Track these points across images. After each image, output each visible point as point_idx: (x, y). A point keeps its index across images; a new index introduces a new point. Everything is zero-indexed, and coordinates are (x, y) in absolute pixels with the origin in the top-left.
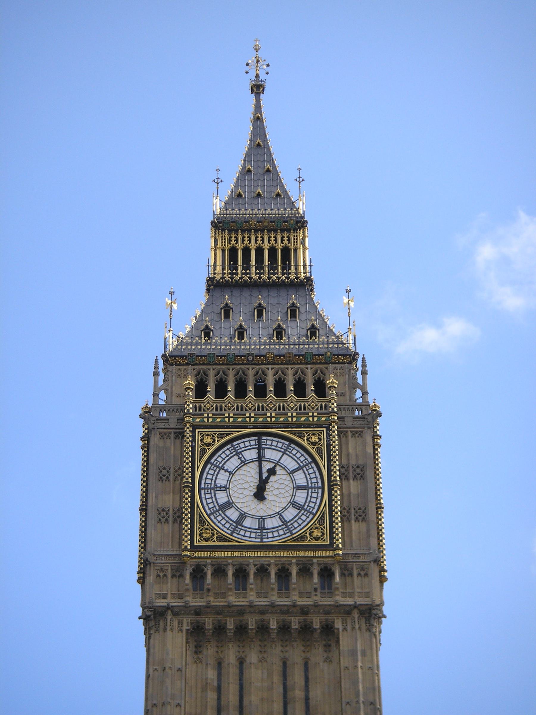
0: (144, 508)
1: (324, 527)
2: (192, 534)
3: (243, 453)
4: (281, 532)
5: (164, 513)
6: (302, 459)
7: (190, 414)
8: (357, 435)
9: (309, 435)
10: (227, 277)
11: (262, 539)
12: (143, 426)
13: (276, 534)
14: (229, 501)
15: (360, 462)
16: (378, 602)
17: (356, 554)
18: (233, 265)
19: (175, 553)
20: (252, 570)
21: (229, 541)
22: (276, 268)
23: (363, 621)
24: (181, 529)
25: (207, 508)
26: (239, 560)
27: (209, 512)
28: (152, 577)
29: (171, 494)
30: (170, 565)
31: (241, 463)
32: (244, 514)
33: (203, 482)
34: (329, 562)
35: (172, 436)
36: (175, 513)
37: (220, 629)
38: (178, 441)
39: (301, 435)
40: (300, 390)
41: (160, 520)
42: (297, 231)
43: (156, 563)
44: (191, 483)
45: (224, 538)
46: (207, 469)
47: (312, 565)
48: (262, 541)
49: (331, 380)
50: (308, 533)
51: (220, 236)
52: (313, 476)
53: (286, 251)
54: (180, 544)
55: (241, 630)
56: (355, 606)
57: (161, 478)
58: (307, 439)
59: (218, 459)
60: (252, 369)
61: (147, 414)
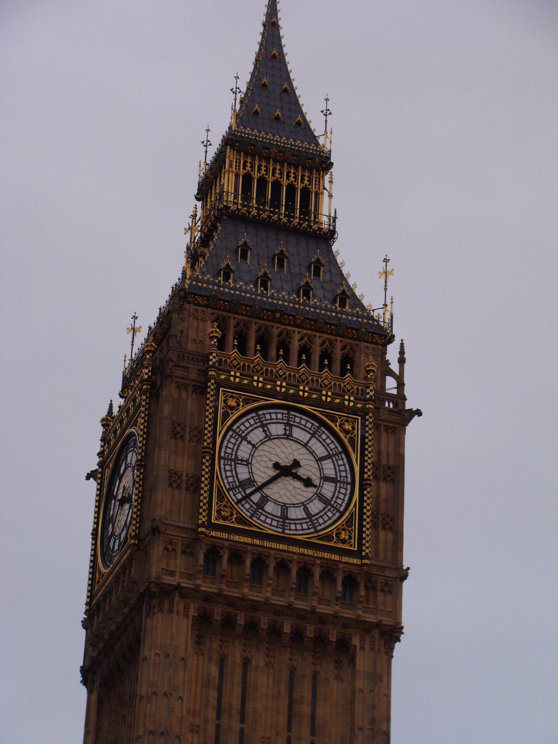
1: (352, 530)
2: (210, 509)
3: (268, 426)
4: (305, 526)
6: (332, 446)
8: (390, 431)
9: (341, 421)
10: (285, 220)
11: (284, 529)
13: (299, 527)
14: (250, 479)
15: (391, 463)
17: (381, 566)
18: (246, 197)
19: (186, 526)
22: (293, 211)
23: (382, 642)
28: (160, 549)
31: (266, 437)
32: (266, 497)
33: (223, 450)
35: (190, 388)
36: (188, 480)
37: (228, 622)
42: (320, 172)
43: (165, 534)
44: (212, 449)
45: (244, 521)
46: (228, 437)
47: (336, 570)
48: (283, 532)
50: (334, 533)
52: (342, 468)
53: (306, 193)
55: (251, 627)
56: (379, 625)
58: (340, 425)
60: (277, 328)
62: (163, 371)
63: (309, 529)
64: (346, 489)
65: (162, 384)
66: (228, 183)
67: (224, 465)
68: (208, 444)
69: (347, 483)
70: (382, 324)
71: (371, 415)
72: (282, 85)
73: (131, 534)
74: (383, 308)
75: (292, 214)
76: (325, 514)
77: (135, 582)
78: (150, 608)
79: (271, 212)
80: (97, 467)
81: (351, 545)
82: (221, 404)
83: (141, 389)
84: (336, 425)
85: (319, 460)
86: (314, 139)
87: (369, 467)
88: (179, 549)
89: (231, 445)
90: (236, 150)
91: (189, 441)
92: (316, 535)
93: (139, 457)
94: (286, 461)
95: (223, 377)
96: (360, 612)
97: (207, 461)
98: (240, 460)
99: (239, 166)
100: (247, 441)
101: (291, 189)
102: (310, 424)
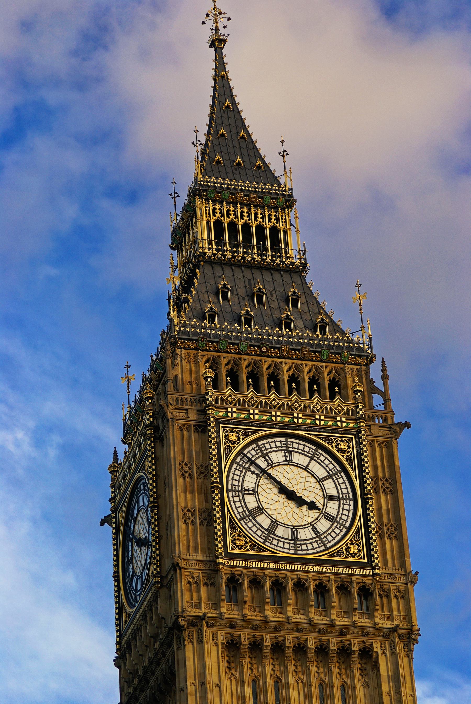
1: (360, 543)
2: (225, 540)
3: (269, 454)
5: (190, 513)
6: (331, 466)
7: (212, 406)
9: (337, 441)
17: (391, 574)
21: (264, 551)
22: (265, 249)
26: (277, 572)
30: (201, 572)
31: (268, 466)
33: (230, 483)
34: (367, 581)
46: (233, 470)
50: (344, 548)
51: (204, 205)
53: (274, 231)
58: (336, 446)
62: (164, 415)
63: (319, 547)
64: (349, 505)
65: (164, 427)
66: (203, 231)
67: (233, 496)
68: (216, 479)
69: (350, 500)
70: (362, 346)
71: (363, 432)
72: (238, 134)
73: (152, 573)
74: (361, 331)
75: (264, 253)
76: (333, 531)
77: (163, 618)
78: (180, 641)
79: (244, 253)
80: (110, 512)
81: (361, 558)
82: (223, 439)
83: (145, 435)
84: (332, 446)
85: (320, 481)
86: (275, 180)
87: (368, 482)
89: (236, 478)
90: (205, 199)
91: (197, 478)
92: (327, 552)
93: (152, 499)
95: (221, 414)
97: (217, 495)
98: (246, 490)
99: (210, 213)
100: (251, 471)
101: (260, 229)
102: (308, 448)
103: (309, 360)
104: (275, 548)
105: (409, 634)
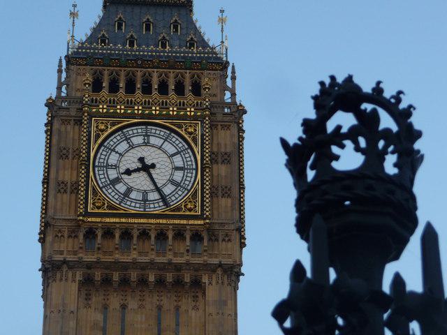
0: (46, 181)
6: (180, 145)
11: (145, 209)
12: (47, 115)
13: (156, 205)
14: (118, 178)
15: (228, 150)
16: (238, 263)
17: (221, 223)
20: (135, 233)
23: (225, 278)
24: (77, 198)
25: (99, 182)
27: (101, 185)
29: (70, 170)
33: (97, 161)
35: (72, 122)
37: (107, 281)
38: (77, 127)
39: (180, 126)
40: (180, 90)
41: (59, 190)
46: (101, 151)
49: (205, 81)
54: (76, 211)
55: (125, 282)
56: (220, 265)
57: (61, 156)
58: (185, 130)
59: (110, 142)
61: (50, 104)
88: (66, 235)
94: (148, 162)
96: (205, 258)
102: (163, 132)
103: (175, 69)
104: (128, 207)
105: (232, 268)
